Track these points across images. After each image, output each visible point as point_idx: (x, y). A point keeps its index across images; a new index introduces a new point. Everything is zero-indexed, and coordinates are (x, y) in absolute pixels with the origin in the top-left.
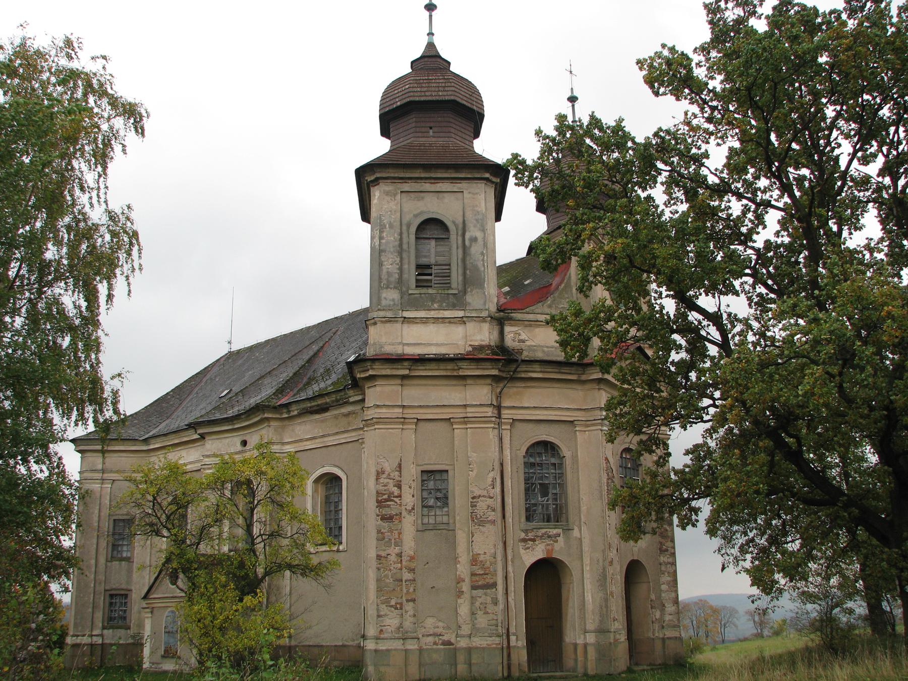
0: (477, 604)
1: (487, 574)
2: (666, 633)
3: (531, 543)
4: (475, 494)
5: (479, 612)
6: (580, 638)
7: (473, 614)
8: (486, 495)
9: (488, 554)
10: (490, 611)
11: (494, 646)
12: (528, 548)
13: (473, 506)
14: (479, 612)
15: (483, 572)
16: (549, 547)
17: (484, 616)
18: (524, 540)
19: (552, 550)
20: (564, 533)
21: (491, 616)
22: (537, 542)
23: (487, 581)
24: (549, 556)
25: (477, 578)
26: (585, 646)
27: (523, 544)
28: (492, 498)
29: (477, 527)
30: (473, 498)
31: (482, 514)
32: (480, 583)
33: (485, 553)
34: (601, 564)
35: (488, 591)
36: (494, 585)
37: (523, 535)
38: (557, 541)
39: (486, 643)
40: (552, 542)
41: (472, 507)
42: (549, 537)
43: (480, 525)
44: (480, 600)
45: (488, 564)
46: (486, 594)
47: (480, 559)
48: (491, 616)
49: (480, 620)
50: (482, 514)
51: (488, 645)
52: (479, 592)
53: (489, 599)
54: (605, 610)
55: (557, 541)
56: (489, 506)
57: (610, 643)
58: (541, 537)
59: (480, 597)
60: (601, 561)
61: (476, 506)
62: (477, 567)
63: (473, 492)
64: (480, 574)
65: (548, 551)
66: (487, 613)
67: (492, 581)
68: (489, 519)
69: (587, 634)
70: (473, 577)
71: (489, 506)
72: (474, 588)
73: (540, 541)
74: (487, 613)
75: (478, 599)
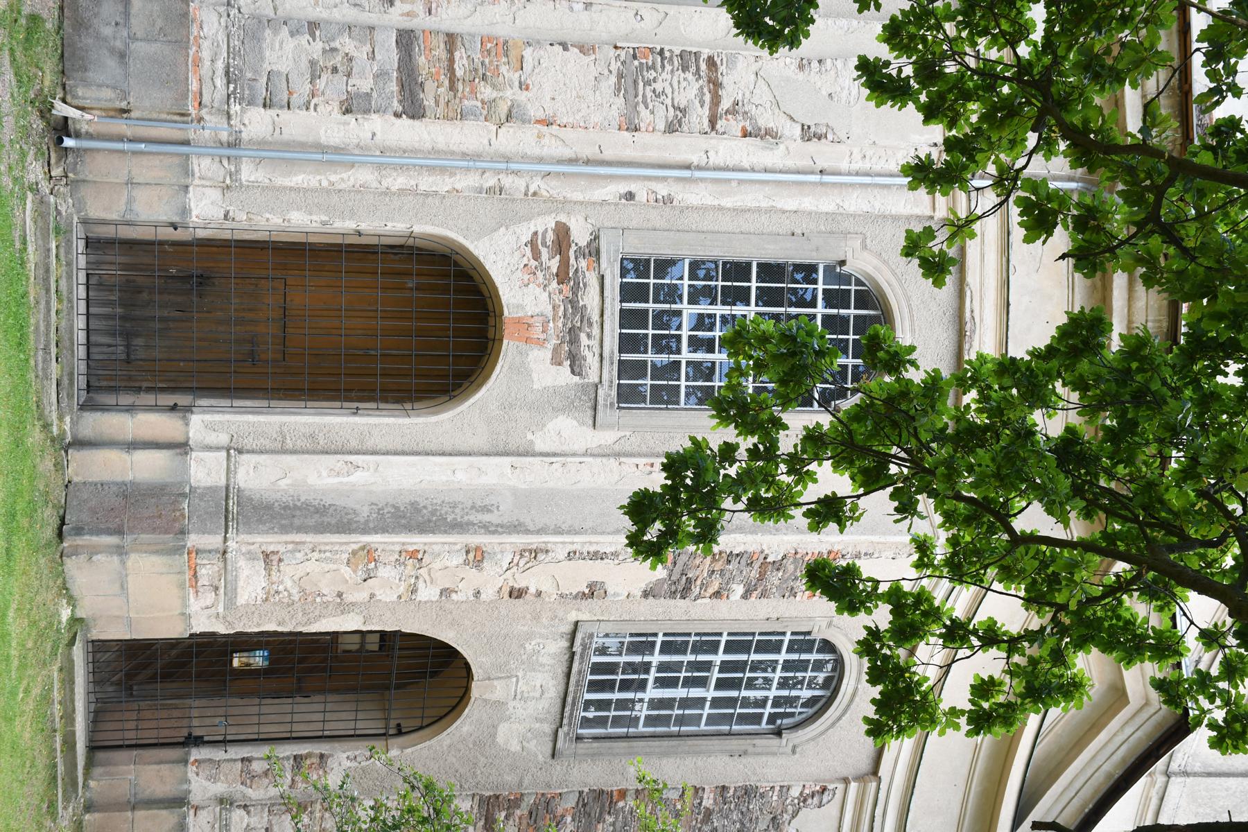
0: (346, 44)
1: (452, 87)
2: (203, 814)
3: (554, 264)
4: (722, 69)
5: (319, 45)
6: (210, 427)
7: (313, 26)
8: (725, 104)
9: (523, 97)
10: (321, 84)
11: (194, 86)
12: (536, 255)
13: (686, 60)
14: (319, 45)
15: (459, 73)
16: (537, 333)
17: (304, 65)
18: (562, 236)
19: (527, 340)
20: (584, 387)
21: (302, 88)
22: (554, 285)
23: (430, 86)
24: (508, 330)
25: (441, 52)
26: (182, 447)
27: (550, 236)
28: (713, 123)
29: (614, 67)
30: (711, 62)
31: (658, 86)
32: (422, 61)
33: (524, 86)
34: (475, 517)
35: (393, 87)
36: (413, 109)
37: (580, 236)
38: (556, 362)
39: (206, 55)
40: (555, 341)
41: (681, 56)
42: (572, 336)
43: (620, 76)
44: (361, 54)
45: (486, 92)
46: (381, 75)
47: (504, 69)
48: (302, 88)
49: (290, 44)
50: (659, 89)
51: (198, 63)
52: (389, 55)
53: (364, 84)
54: (311, 522)
55: (556, 362)
56: (684, 111)
57: (183, 532)
58: (573, 302)
59: (372, 56)
60: (486, 518)
61: (685, 68)
62: (477, 57)
63: (732, 61)
64: (451, 61)
65: (524, 324)
66: (314, 77)
67: (429, 102)
68: (641, 107)
69: (224, 454)
70: (442, 38)
71: (684, 111)
72: (406, 40)
73: (558, 299)
74: (314, 77)
75: (368, 48)
